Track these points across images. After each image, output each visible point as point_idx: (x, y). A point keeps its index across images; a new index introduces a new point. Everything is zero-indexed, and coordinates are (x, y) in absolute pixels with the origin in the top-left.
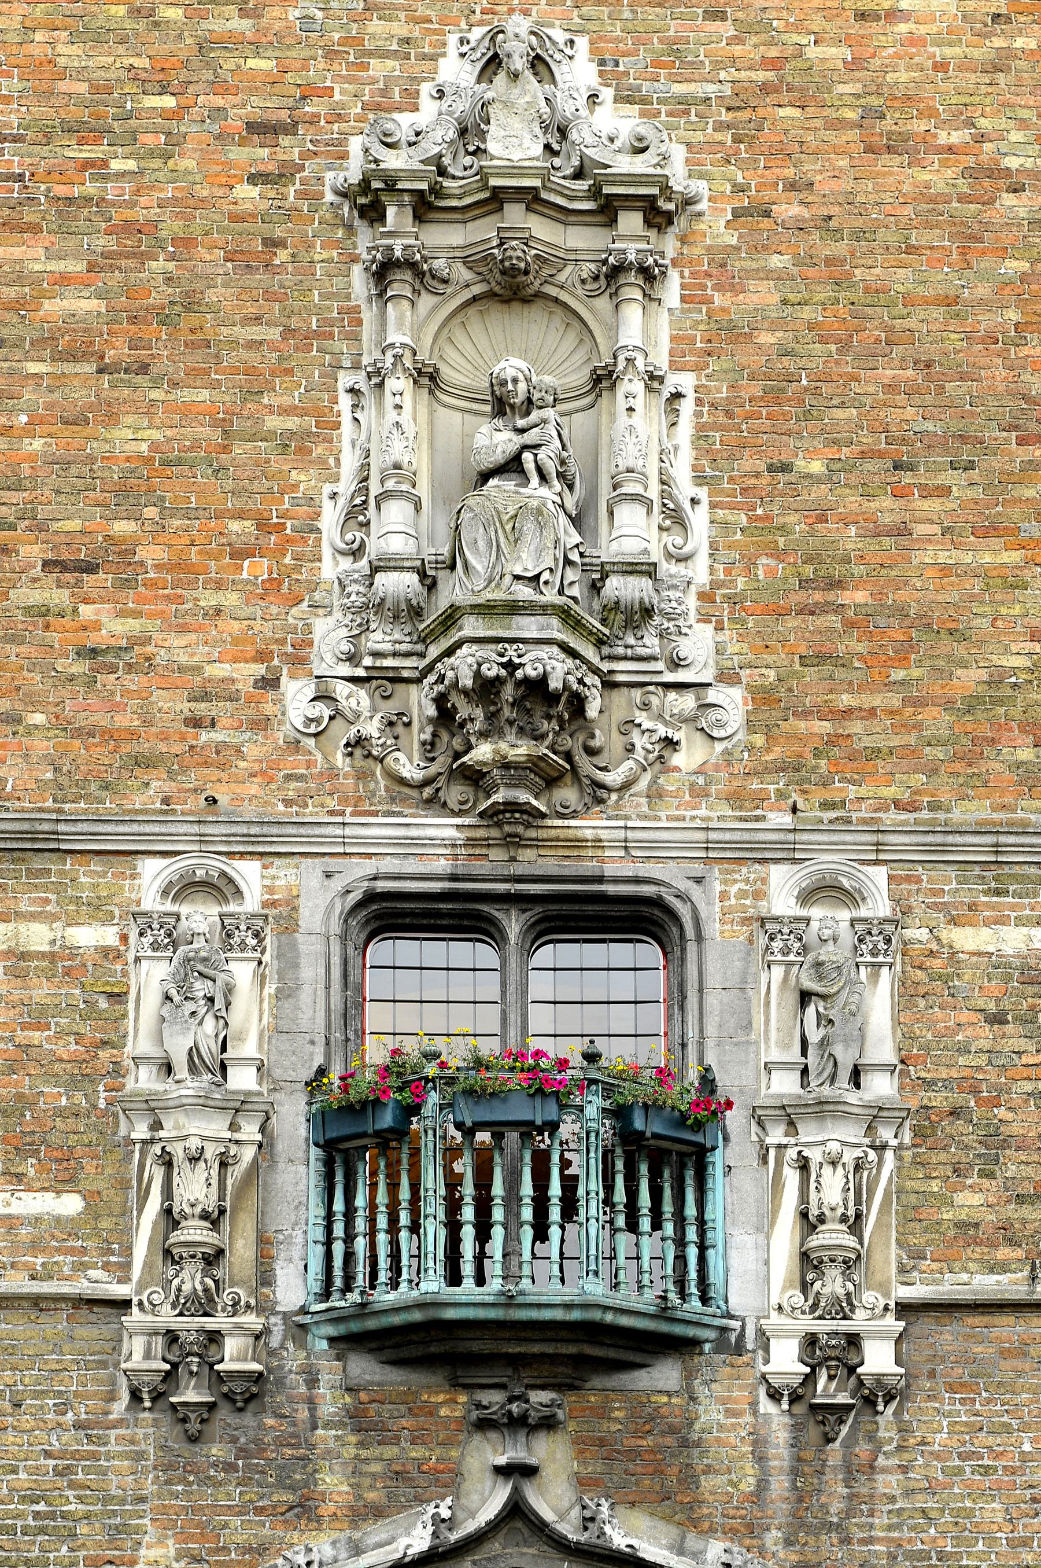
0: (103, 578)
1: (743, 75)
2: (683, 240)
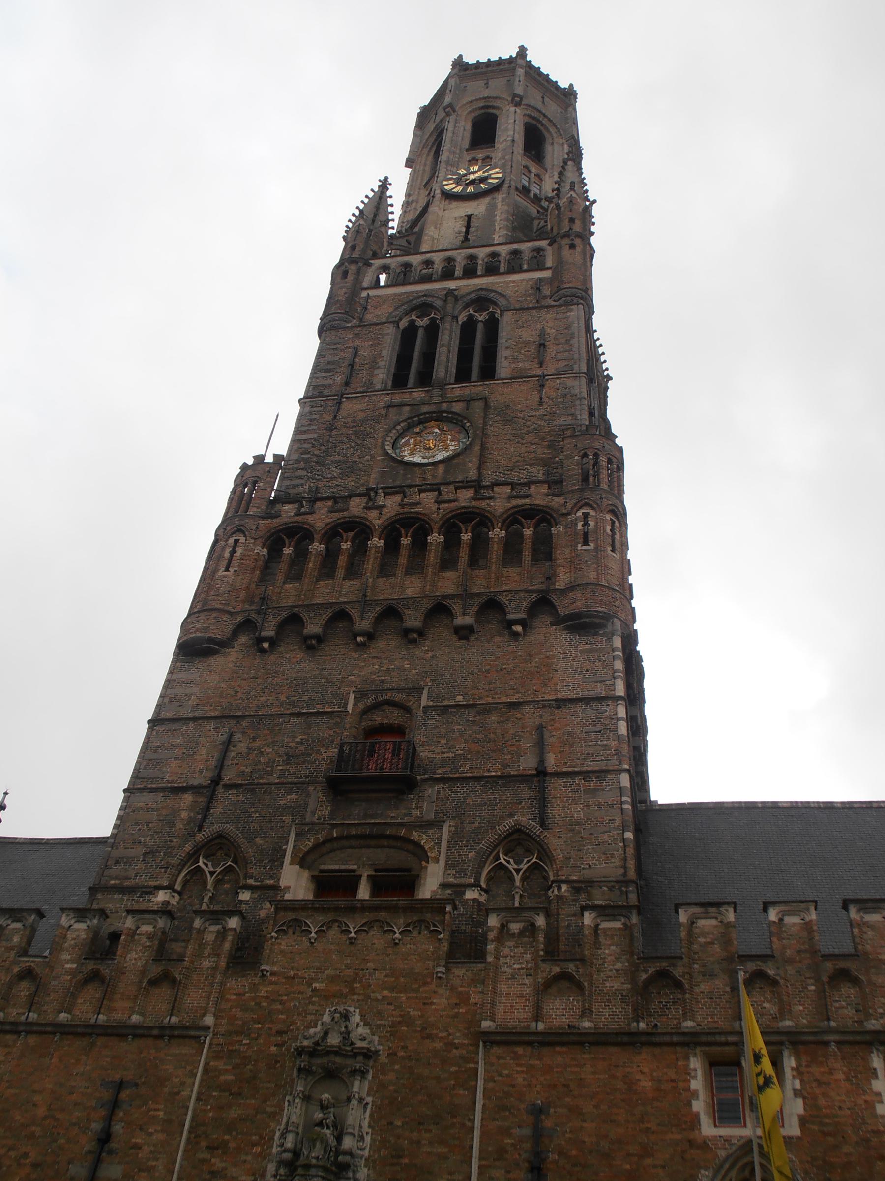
0: (220, 1151)
1: (394, 1019)
2: (375, 1062)
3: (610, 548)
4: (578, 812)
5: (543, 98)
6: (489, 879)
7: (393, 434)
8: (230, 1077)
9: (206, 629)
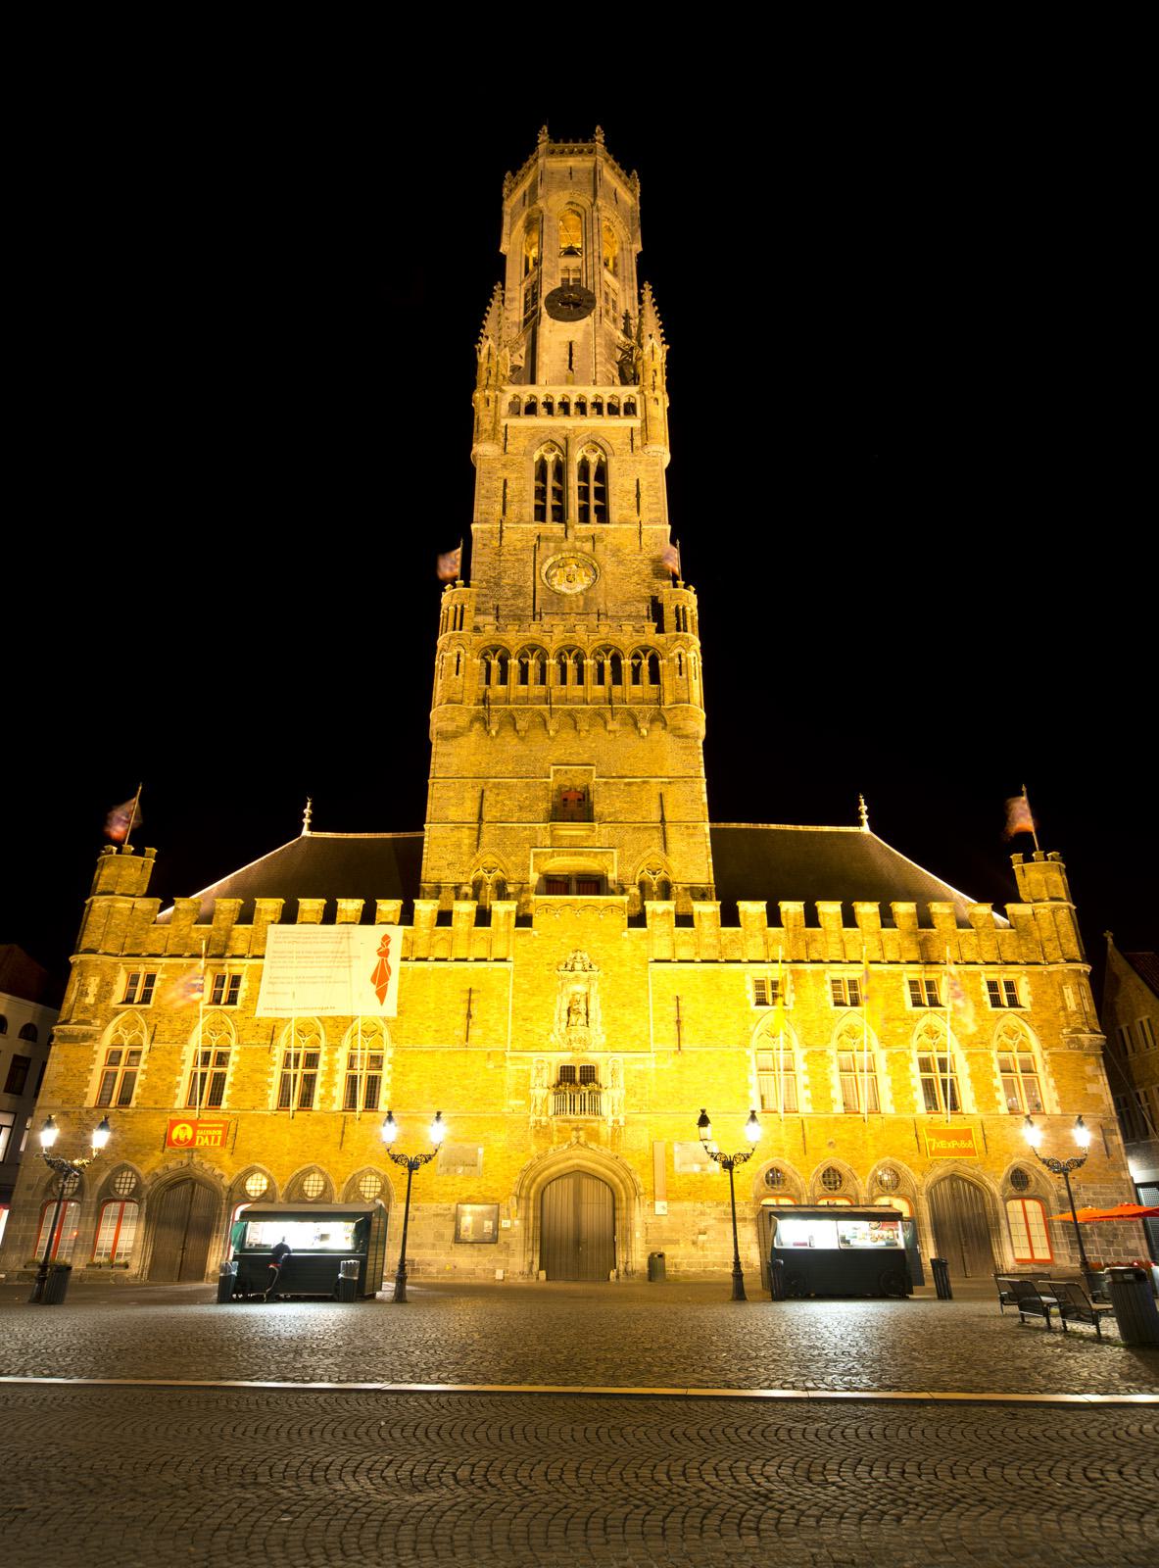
8: (527, 987)
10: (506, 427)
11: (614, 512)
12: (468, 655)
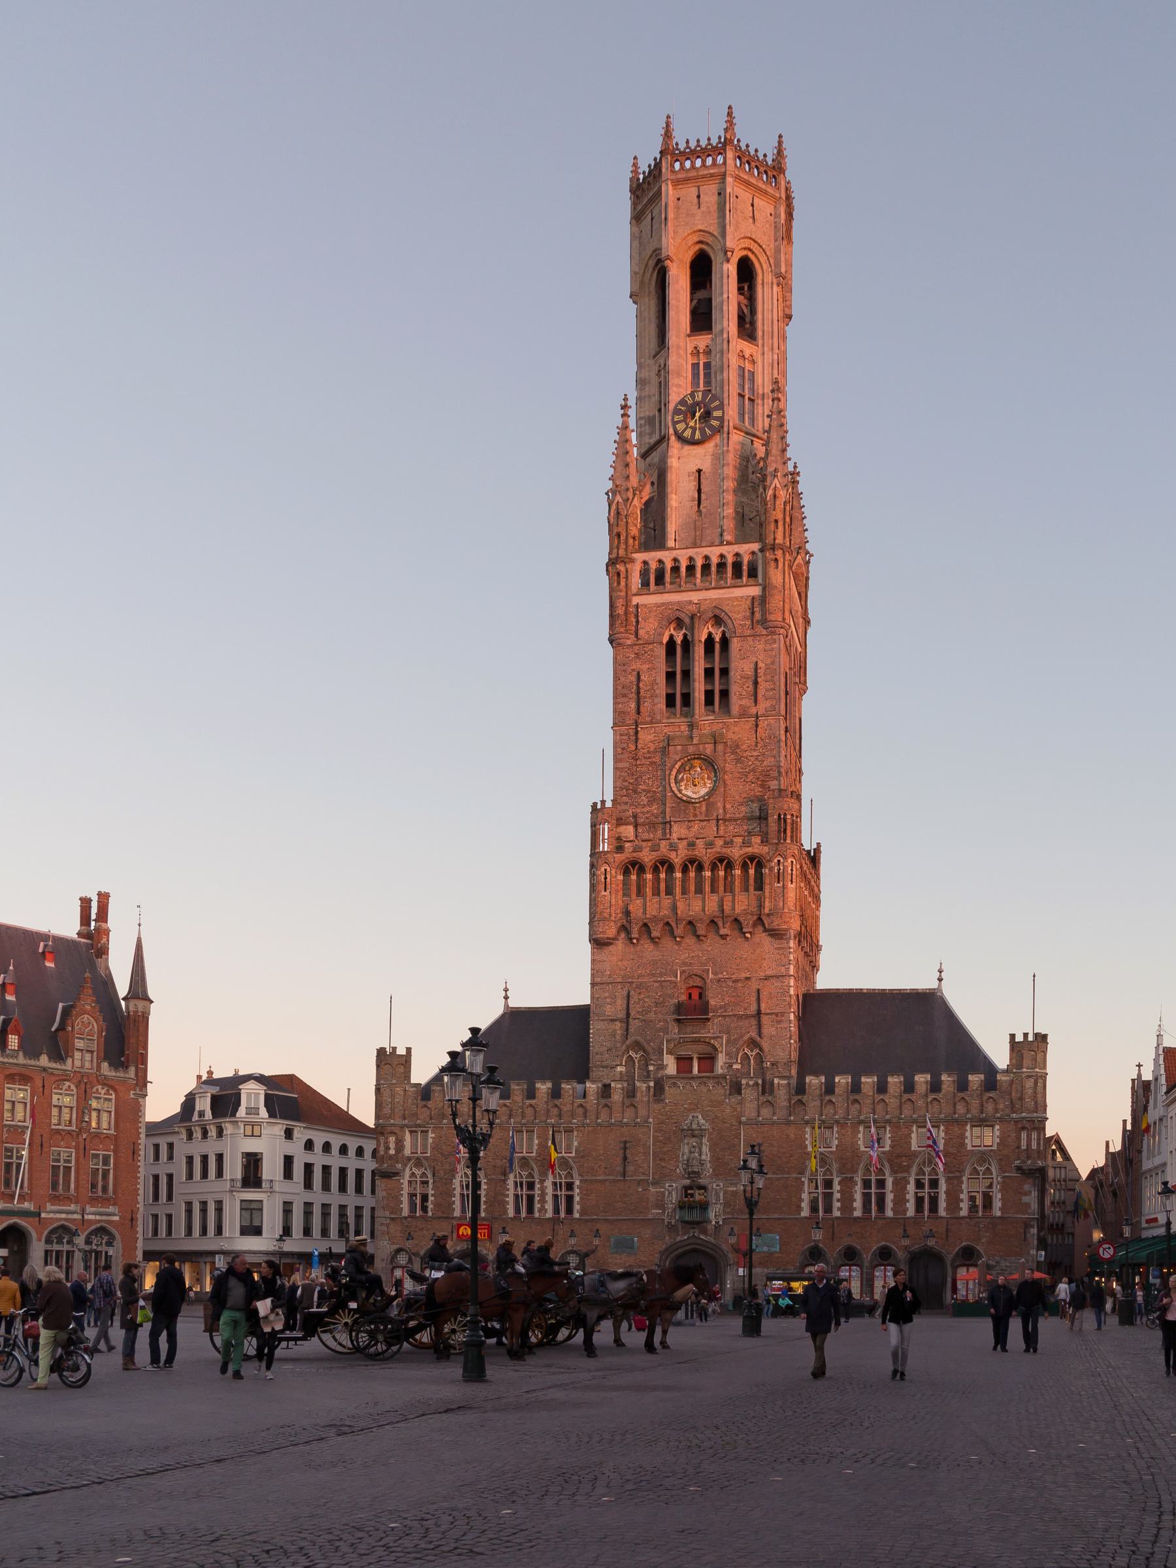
3: (790, 883)
4: (773, 1031)
5: (752, 205)
6: (741, 1058)
7: (674, 772)
9: (604, 932)
10: (637, 606)
11: (736, 703)
12: (613, 872)
